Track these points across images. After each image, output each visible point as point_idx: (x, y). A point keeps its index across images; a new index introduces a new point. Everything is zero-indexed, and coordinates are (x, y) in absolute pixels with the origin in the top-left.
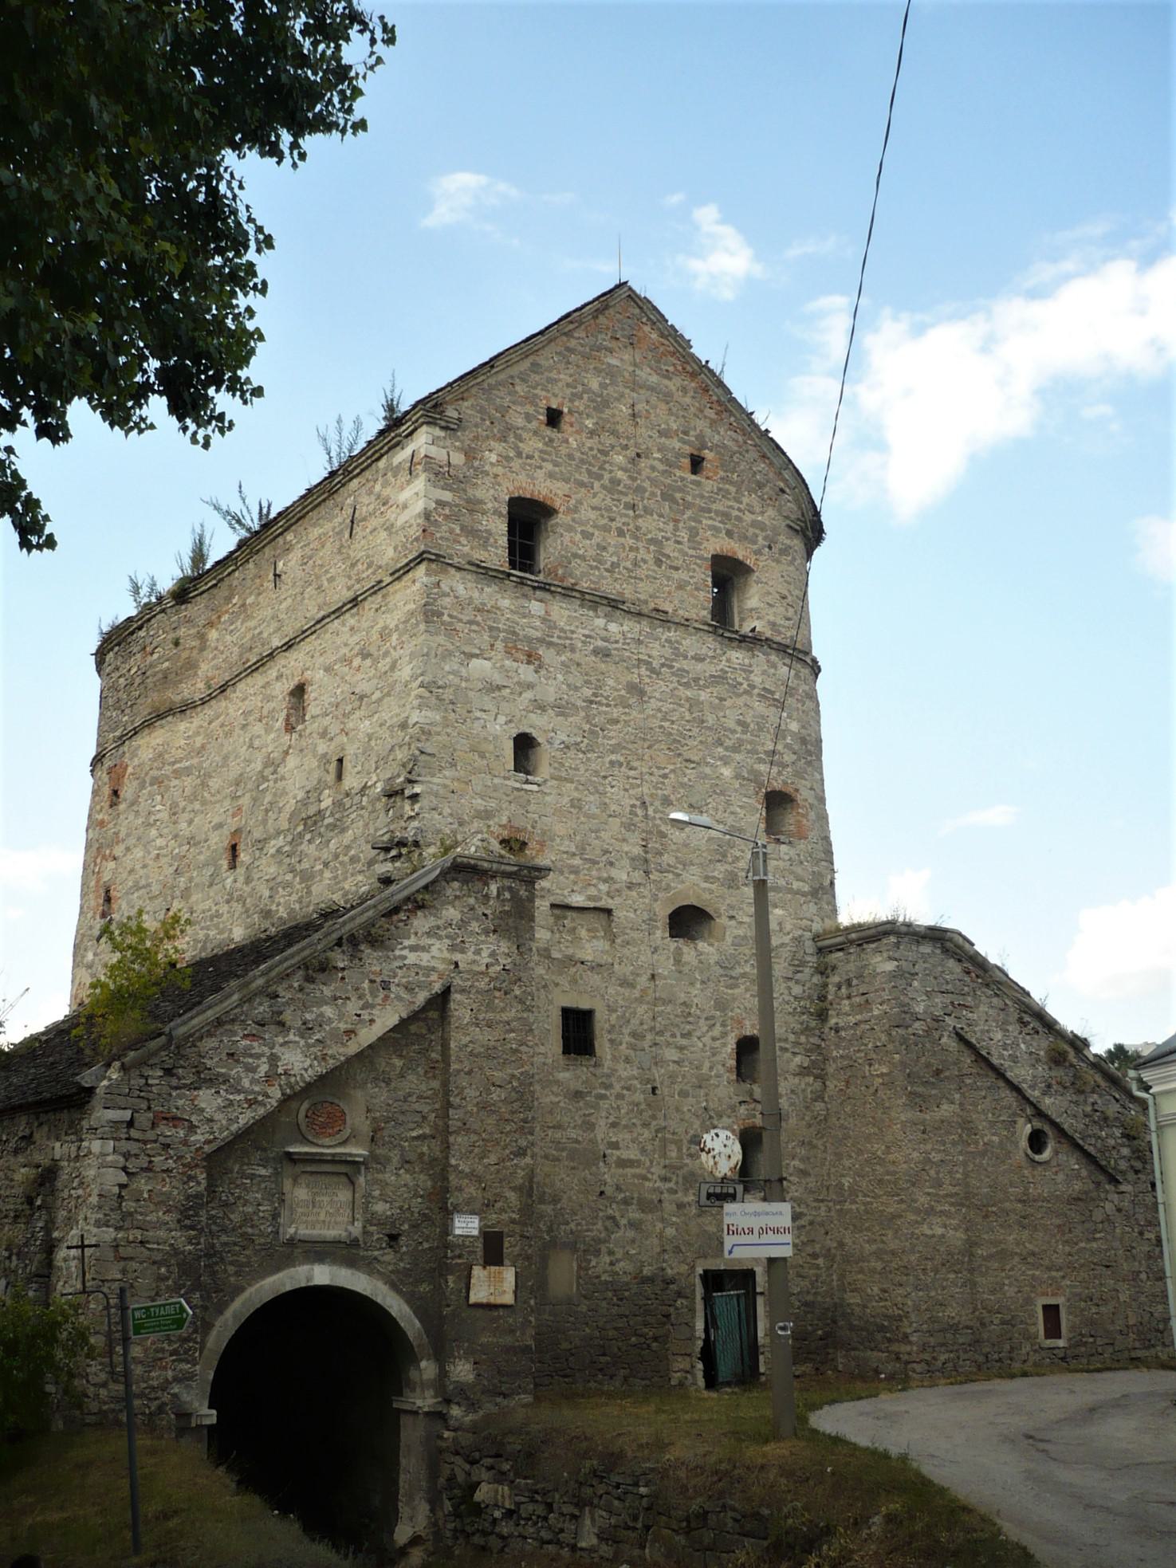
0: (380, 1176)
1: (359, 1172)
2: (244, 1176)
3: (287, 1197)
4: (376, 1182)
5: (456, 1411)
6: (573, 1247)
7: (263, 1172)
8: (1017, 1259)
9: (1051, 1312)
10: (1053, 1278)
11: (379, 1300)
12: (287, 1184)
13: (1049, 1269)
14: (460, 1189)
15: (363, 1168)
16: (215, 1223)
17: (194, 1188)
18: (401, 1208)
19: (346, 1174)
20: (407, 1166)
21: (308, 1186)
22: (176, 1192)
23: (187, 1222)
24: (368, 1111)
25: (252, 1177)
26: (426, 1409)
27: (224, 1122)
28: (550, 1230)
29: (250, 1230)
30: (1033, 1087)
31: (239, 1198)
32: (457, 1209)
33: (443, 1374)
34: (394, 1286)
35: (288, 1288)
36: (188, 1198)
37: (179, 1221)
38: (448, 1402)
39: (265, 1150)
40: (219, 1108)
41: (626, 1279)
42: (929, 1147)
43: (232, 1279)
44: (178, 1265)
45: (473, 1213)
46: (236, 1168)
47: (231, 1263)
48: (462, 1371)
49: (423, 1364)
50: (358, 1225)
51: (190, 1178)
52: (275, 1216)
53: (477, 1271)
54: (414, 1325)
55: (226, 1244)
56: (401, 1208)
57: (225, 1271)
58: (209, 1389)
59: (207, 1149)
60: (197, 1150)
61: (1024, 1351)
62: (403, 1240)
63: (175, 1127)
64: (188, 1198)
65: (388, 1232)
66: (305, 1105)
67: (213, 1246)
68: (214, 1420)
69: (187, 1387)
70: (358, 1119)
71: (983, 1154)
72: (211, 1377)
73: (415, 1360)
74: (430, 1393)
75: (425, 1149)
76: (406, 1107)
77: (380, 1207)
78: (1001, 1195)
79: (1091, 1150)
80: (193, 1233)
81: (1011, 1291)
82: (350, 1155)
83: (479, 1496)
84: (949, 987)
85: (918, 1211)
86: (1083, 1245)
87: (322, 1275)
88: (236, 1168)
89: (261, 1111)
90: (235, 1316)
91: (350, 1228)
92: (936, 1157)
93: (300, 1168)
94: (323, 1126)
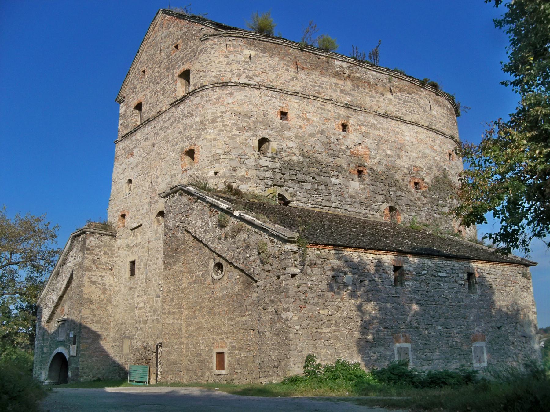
6: (128, 337)
8: (206, 330)
9: (221, 355)
10: (222, 339)
13: (221, 334)
28: (124, 333)
30: (212, 243)
41: (140, 347)
42: (170, 285)
53: (71, 347)
61: (206, 376)
71: (195, 282)
78: (200, 300)
79: (241, 266)
81: (202, 347)
84: (183, 210)
85: (165, 313)
86: (238, 319)
92: (172, 288)
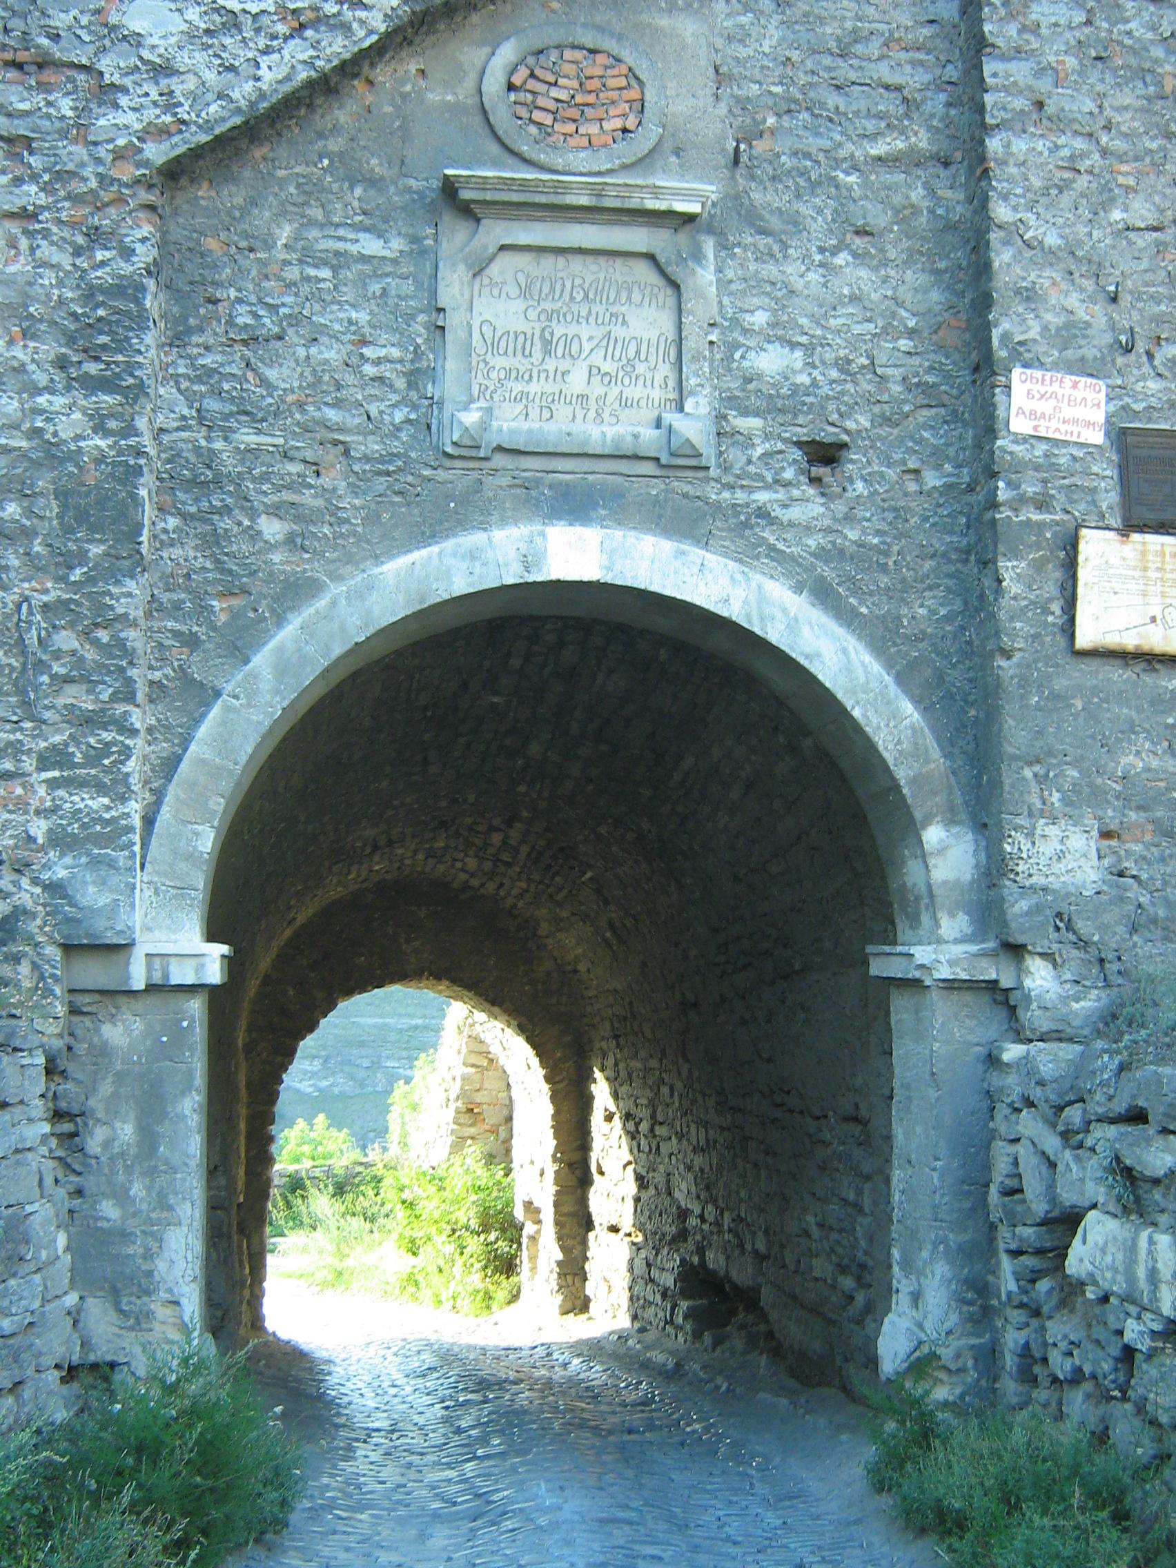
0: (770, 270)
1: (698, 256)
2: (308, 257)
3: (453, 321)
4: (754, 284)
5: (1040, 978)
7: (371, 245)
11: (775, 635)
12: (453, 286)
14: (1029, 296)
15: (709, 246)
16: (218, 393)
17: (107, 267)
18: (843, 365)
19: (651, 257)
20: (859, 243)
21: (525, 293)
22: (49, 278)
23: (92, 368)
24: (721, 77)
25: (338, 262)
26: (944, 973)
27: (210, 76)
29: (332, 414)
31: (295, 320)
32: (1023, 355)
33: (995, 869)
34: (823, 595)
35: (461, 585)
36: (90, 294)
37: (62, 363)
38: (1015, 951)
39: (373, 182)
40: (191, 35)
43: (276, 557)
44: (62, 495)
45: (1082, 368)
46: (284, 233)
47: (276, 511)
48: (1061, 855)
49: (933, 835)
50: (700, 404)
51: (96, 236)
52: (418, 375)
53: (1096, 547)
54: (896, 715)
55: (252, 453)
56: (843, 365)
57: (254, 535)
58: (200, 881)
59: (157, 153)
60: (119, 155)
62: (854, 462)
63: (44, 87)
64: (90, 294)
65: (803, 433)
66: (507, 53)
67: (209, 459)
68: (214, 974)
69: (95, 862)
70: (684, 98)
72: (207, 841)
73: (911, 830)
74: (953, 925)
75: (917, 195)
76: (846, 71)
77: (770, 361)
80: (108, 399)
82: (656, 191)
83: (1079, 1259)
87: (575, 553)
88: (284, 233)
89: (337, 48)
90: (281, 670)
91: (670, 417)
93: (496, 232)
94: (574, 111)
